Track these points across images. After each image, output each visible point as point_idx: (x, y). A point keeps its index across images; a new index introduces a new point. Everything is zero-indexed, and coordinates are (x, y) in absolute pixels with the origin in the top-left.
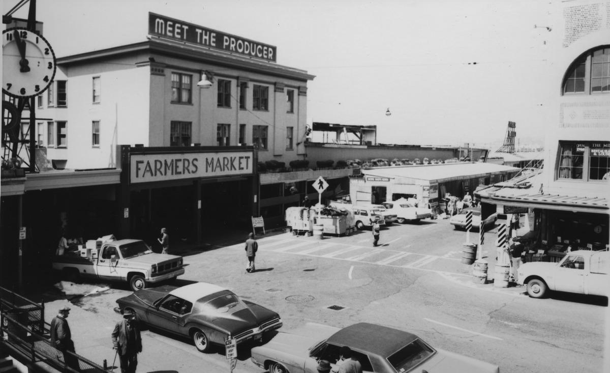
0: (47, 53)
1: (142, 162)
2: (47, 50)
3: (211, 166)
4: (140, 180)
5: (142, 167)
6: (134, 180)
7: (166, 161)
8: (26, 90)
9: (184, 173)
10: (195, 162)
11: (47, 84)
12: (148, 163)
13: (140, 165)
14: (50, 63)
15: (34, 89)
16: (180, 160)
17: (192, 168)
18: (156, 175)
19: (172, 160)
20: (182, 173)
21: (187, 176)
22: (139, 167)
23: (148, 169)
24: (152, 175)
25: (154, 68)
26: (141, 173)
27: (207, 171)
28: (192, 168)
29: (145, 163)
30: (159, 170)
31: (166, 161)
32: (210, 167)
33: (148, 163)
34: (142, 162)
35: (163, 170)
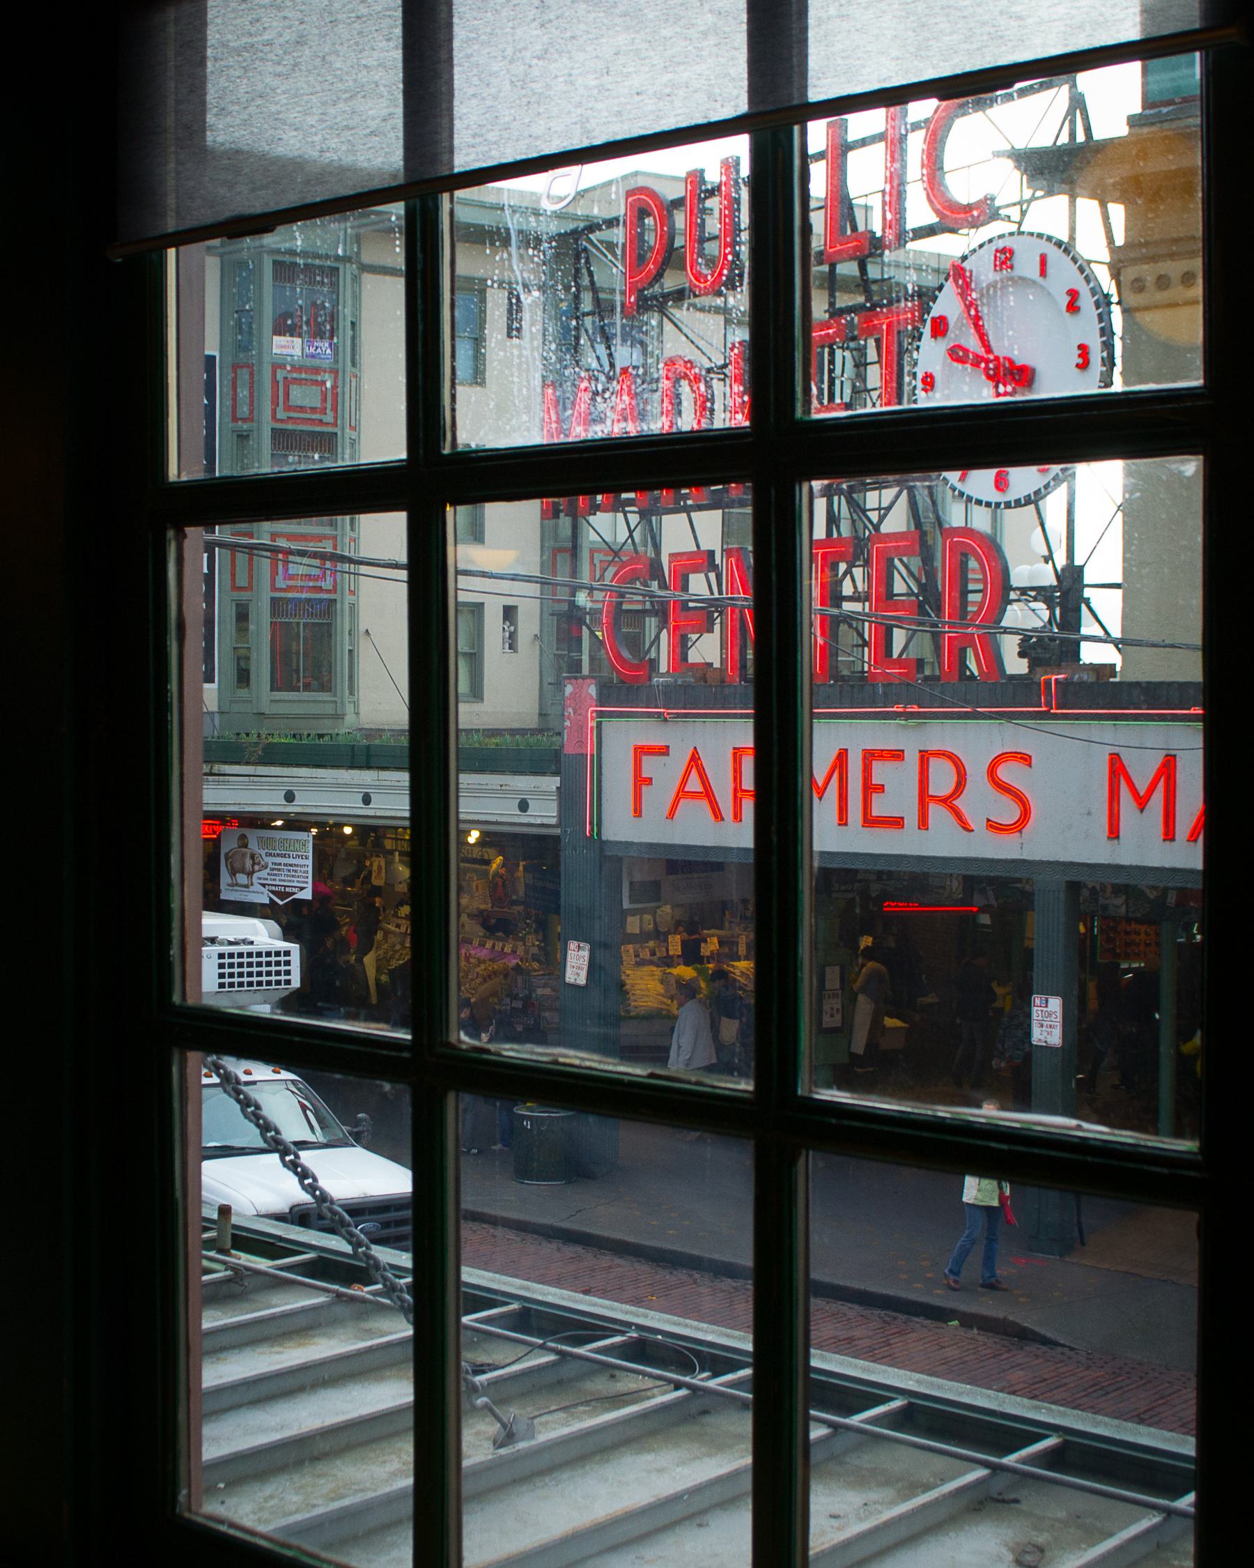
0: (1073, 307)
1: (664, 751)
2: (1074, 294)
5: (666, 775)
6: (620, 825)
9: (923, 823)
10: (1007, 773)
12: (695, 759)
13: (650, 765)
14: (1084, 350)
16: (897, 755)
17: (981, 801)
19: (842, 756)
20: (912, 819)
21: (941, 841)
22: (645, 774)
23: (694, 784)
24: (718, 815)
27: (1114, 833)
28: (981, 801)
29: (679, 759)
32: (1142, 802)
33: (695, 759)
34: (664, 751)
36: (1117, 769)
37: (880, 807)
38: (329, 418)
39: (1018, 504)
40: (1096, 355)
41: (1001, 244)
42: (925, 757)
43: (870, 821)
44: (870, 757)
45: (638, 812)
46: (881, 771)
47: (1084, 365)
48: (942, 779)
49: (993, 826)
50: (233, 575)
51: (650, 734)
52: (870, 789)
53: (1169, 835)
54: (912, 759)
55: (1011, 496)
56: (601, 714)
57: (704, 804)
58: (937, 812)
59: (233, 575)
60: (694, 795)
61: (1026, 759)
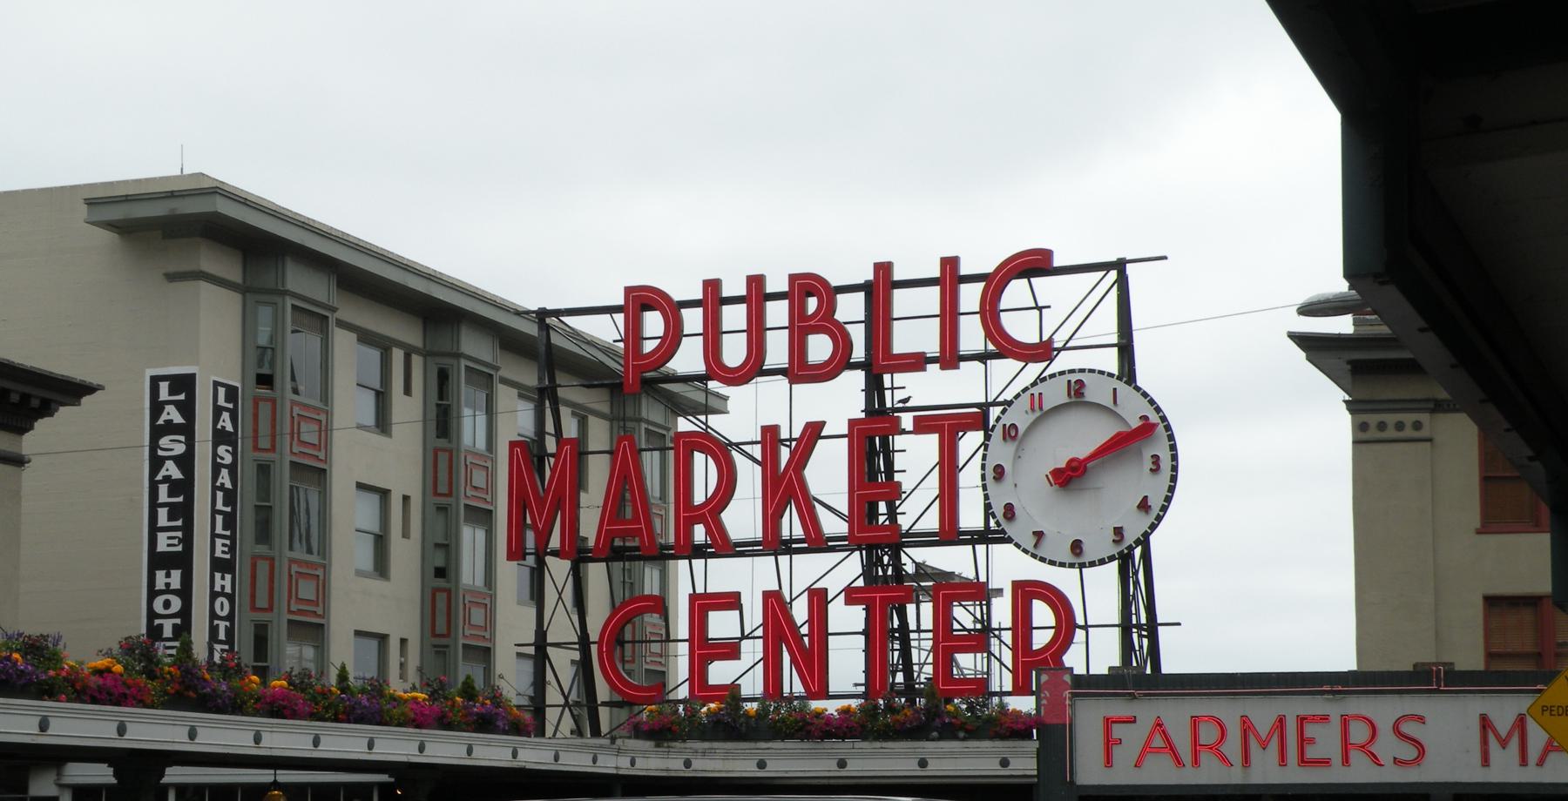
1: (1132, 720)
3: (1514, 743)
4: (1123, 774)
7: (1245, 721)
8: (1085, 547)
9: (1346, 761)
10: (1407, 728)
11: (1151, 519)
13: (1118, 732)
15: (1113, 537)
16: (1325, 719)
17: (1388, 746)
18: (1196, 762)
19: (1281, 721)
20: (1337, 758)
21: (1360, 773)
23: (1158, 742)
24: (1179, 761)
25: (1373, 419)
26: (1124, 756)
27: (1486, 761)
28: (1388, 746)
30: (1214, 748)
31: (1245, 721)
33: (1159, 725)
34: (1132, 720)
35: (1232, 747)
36: (1485, 723)
37: (1311, 753)
38: (322, 456)
39: (1092, 564)
40: (1166, 463)
41: (1074, 378)
42: (1345, 721)
43: (1303, 761)
44: (1302, 720)
45: (1109, 762)
46: (1311, 730)
47: (1156, 470)
48: (1359, 733)
49: (1396, 761)
50: (253, 597)
51: (1118, 708)
52: (1303, 741)
53: (1524, 761)
54: (1336, 721)
55: (1086, 559)
56: (1074, 695)
57: (1166, 760)
58: (1355, 755)
59: (253, 597)
60: (1158, 750)
61: (1421, 719)
